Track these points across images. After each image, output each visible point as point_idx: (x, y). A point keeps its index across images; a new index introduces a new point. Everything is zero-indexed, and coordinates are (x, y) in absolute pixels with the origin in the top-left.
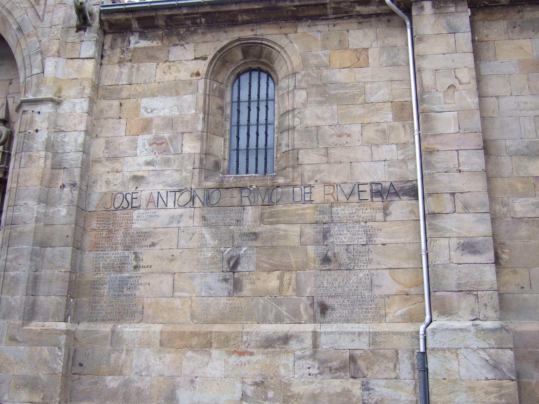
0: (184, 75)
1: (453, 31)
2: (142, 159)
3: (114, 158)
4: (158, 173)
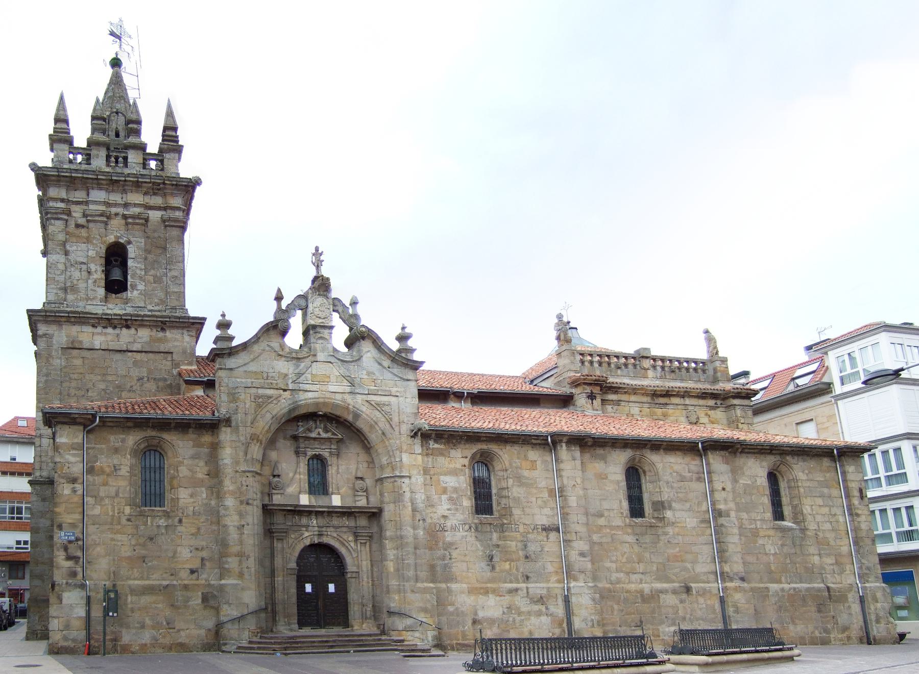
0: (459, 466)
2: (446, 506)
3: (433, 506)
4: (454, 515)
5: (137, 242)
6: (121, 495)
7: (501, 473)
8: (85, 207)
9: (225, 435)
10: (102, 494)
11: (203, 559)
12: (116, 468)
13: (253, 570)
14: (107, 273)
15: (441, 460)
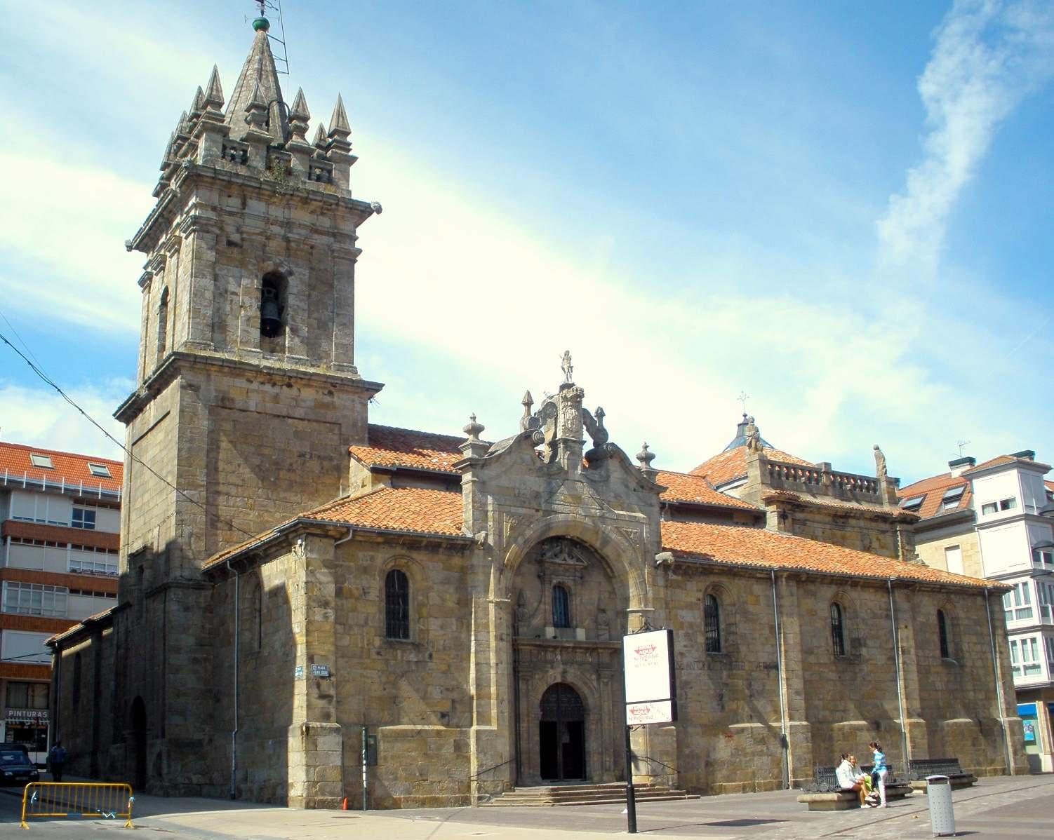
0: (694, 600)
1: (792, 595)
5: (300, 274)
6: (370, 624)
7: (729, 608)
8: (240, 221)
9: (478, 558)
10: (351, 622)
11: (453, 701)
12: (365, 592)
13: (506, 714)
14: (262, 309)
15: (678, 591)
